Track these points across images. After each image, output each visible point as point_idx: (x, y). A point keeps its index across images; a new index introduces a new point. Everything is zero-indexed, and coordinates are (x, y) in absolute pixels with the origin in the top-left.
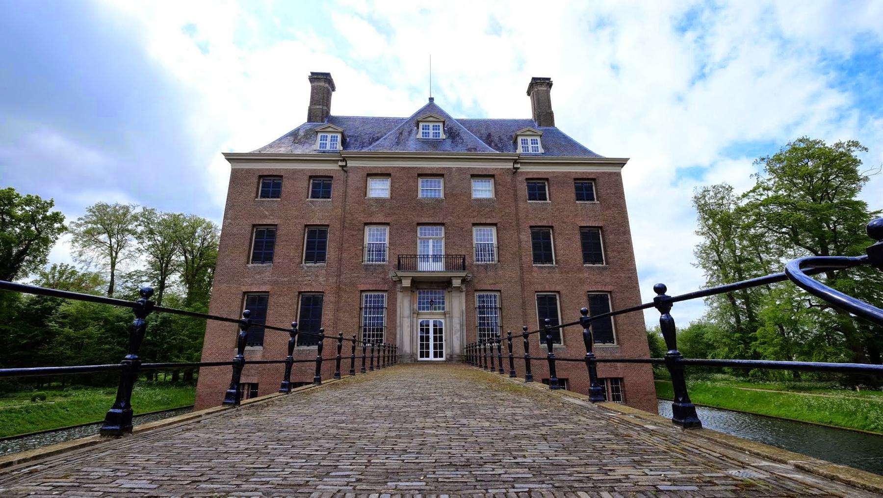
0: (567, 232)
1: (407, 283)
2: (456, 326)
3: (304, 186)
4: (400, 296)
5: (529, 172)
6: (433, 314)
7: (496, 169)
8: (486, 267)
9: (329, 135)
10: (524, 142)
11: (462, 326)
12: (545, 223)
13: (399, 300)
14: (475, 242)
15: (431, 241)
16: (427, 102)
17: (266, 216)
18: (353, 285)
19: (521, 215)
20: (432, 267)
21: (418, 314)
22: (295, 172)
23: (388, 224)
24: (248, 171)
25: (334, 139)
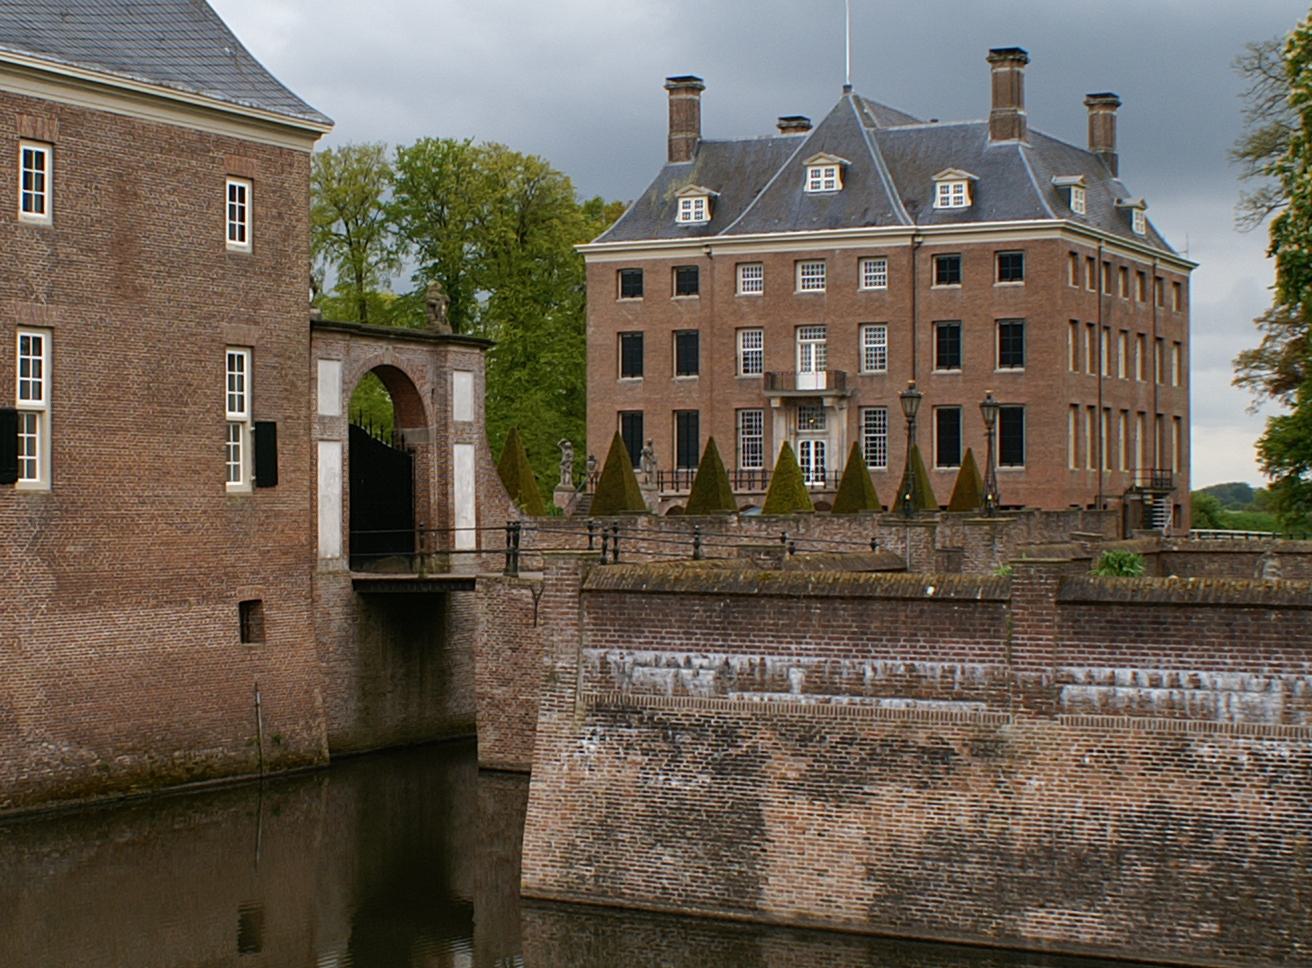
0: (978, 328)
1: (775, 403)
2: (835, 448)
3: (668, 280)
4: (775, 413)
5: (936, 246)
6: (813, 433)
7: (889, 248)
8: (872, 377)
9: (693, 201)
10: (945, 190)
11: (841, 448)
12: (951, 317)
13: (775, 419)
14: (864, 346)
15: (813, 347)
16: (840, 96)
17: (629, 322)
18: (727, 403)
19: (921, 307)
20: (811, 381)
21: (797, 434)
22: (655, 262)
23: (761, 327)
24: (605, 264)
25: (698, 204)
